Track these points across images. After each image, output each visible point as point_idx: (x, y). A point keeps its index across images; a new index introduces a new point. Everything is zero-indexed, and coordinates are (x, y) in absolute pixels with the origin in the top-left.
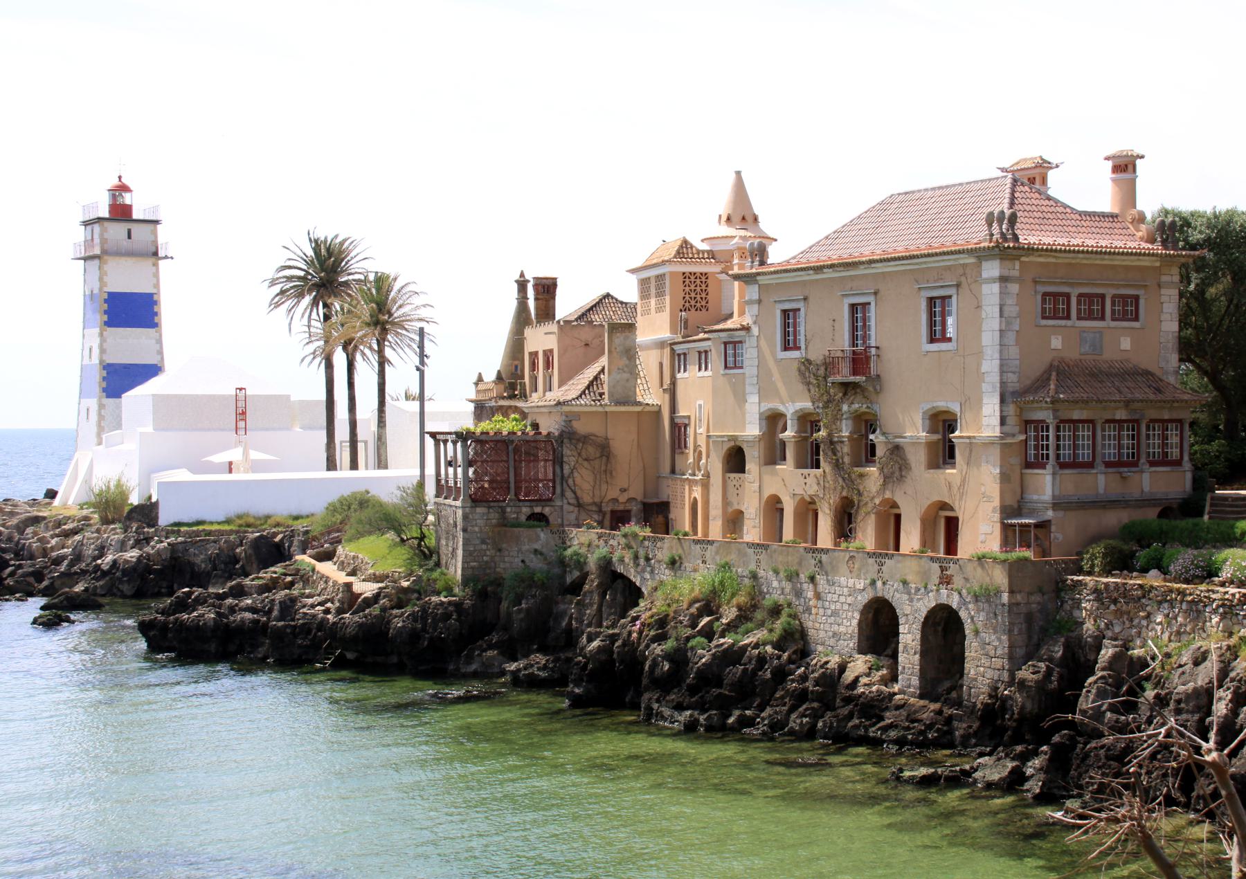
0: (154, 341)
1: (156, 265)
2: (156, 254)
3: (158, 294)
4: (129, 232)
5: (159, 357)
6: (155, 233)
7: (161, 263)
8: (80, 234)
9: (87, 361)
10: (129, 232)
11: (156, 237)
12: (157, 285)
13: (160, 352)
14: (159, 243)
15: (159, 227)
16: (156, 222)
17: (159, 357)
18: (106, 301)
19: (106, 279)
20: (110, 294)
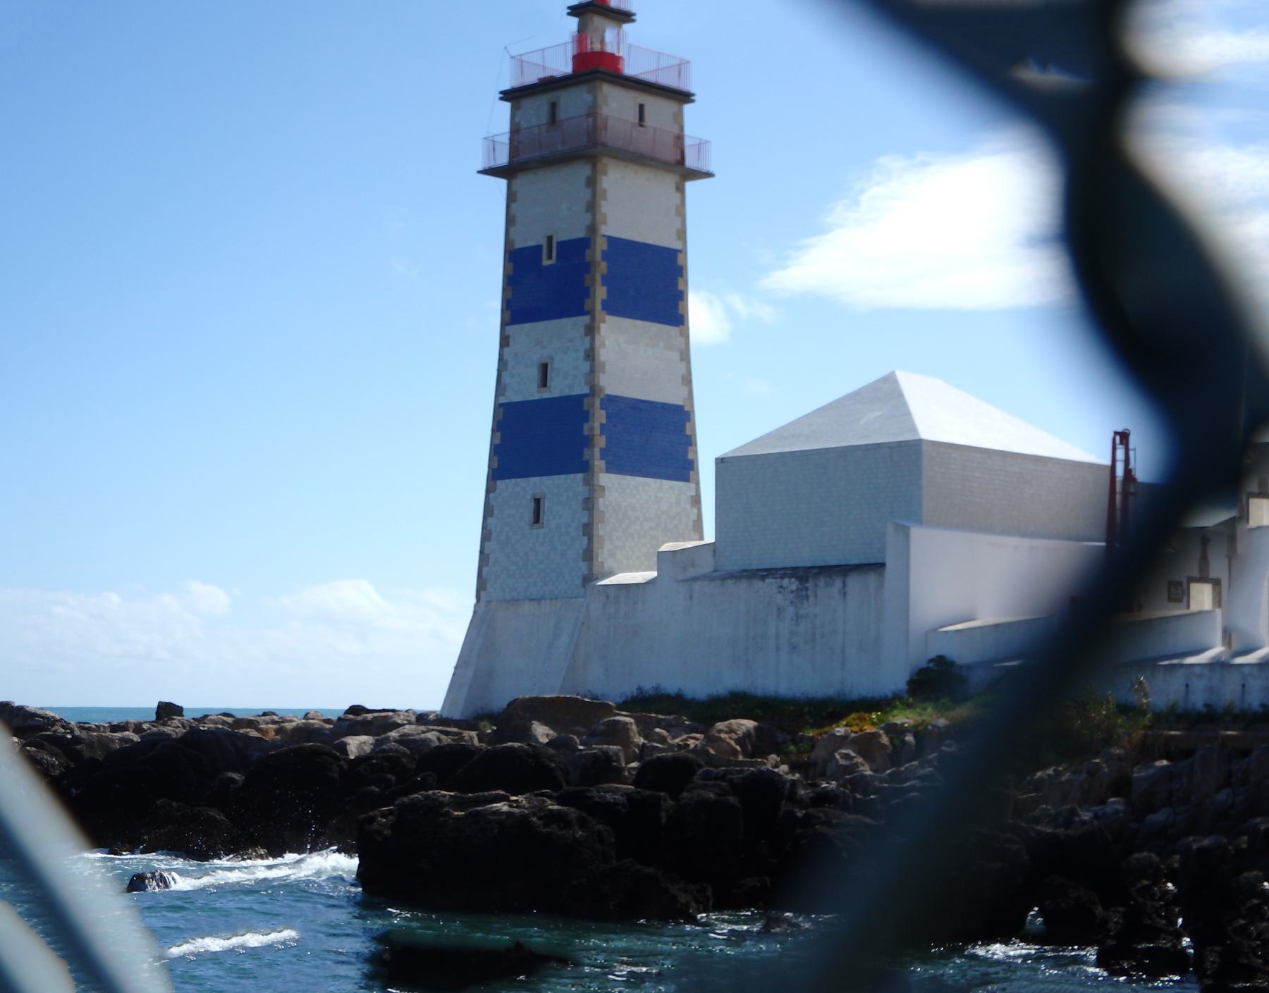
0: (676, 356)
1: (680, 190)
2: (681, 161)
3: (683, 251)
4: (641, 107)
5: (685, 391)
6: (679, 119)
7: (691, 187)
8: (500, 118)
9: (512, 397)
10: (641, 107)
11: (682, 128)
12: (682, 234)
13: (687, 380)
14: (687, 142)
15: (687, 108)
16: (684, 97)
17: (685, 391)
18: (606, 256)
19: (605, 207)
20: (612, 240)
